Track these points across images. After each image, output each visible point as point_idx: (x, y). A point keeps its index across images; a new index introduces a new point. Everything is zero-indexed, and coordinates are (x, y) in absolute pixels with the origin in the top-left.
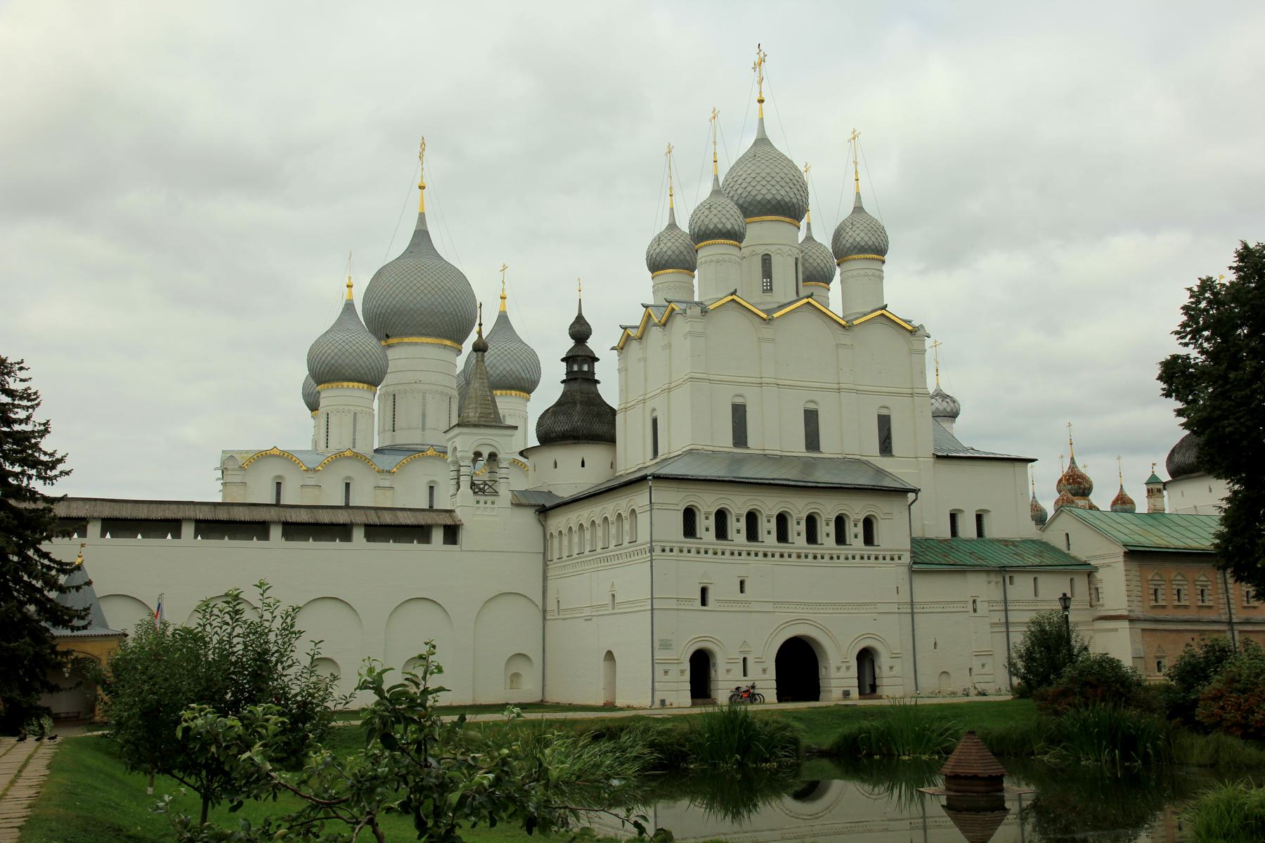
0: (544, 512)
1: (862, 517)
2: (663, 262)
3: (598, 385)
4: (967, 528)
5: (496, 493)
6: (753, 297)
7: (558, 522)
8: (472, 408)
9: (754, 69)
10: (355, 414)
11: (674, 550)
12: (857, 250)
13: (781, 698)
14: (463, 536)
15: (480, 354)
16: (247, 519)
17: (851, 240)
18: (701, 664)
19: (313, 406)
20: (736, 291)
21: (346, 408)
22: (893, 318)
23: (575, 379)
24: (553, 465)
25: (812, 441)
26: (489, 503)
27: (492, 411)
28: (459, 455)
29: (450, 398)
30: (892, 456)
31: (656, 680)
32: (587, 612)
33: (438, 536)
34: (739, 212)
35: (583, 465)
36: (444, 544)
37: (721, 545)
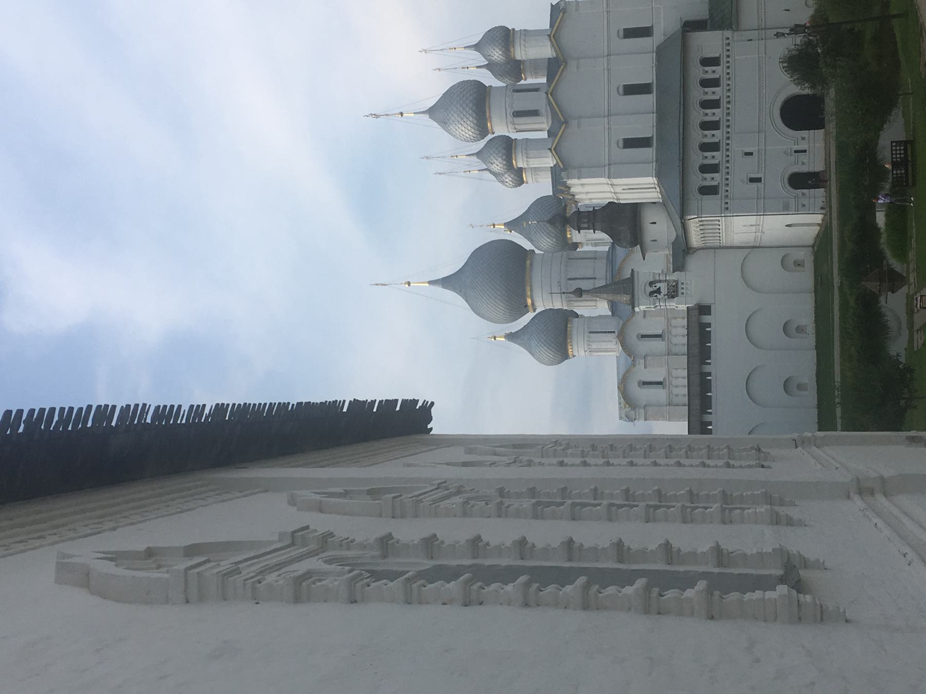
2: (518, 179)
5: (677, 282)
7: (695, 240)
8: (621, 298)
11: (726, 201)
12: (508, 52)
17: (502, 57)
18: (799, 181)
20: (548, 149)
25: (643, 89)
27: (622, 286)
29: (570, 259)
30: (652, 26)
33: (706, 319)
35: (655, 223)
36: (710, 315)
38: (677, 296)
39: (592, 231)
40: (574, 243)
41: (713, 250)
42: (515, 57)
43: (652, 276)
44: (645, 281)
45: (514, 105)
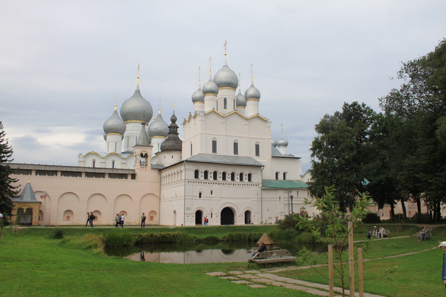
0: (160, 170)
1: (248, 173)
2: (196, 100)
3: (178, 135)
4: (281, 177)
5: (147, 165)
6: (221, 110)
7: (164, 174)
9: (224, 46)
10: (116, 142)
11: (192, 182)
13: (221, 224)
14: (137, 177)
15: (143, 125)
16: (75, 171)
17: (249, 95)
18: (199, 214)
19: (106, 139)
21: (114, 140)
22: (261, 117)
23: (172, 133)
24: (164, 157)
25: (236, 151)
26: (145, 168)
27: (146, 142)
28: (136, 154)
30: (260, 156)
31: (185, 218)
32: (170, 199)
33: (129, 177)
34: (216, 86)
35: (172, 157)
37: (206, 181)
38: (141, 165)
39: (169, 132)
40: (151, 139)
41: (160, 181)
42: (249, 100)
43: (150, 155)
44: (147, 151)
45: (229, 99)
